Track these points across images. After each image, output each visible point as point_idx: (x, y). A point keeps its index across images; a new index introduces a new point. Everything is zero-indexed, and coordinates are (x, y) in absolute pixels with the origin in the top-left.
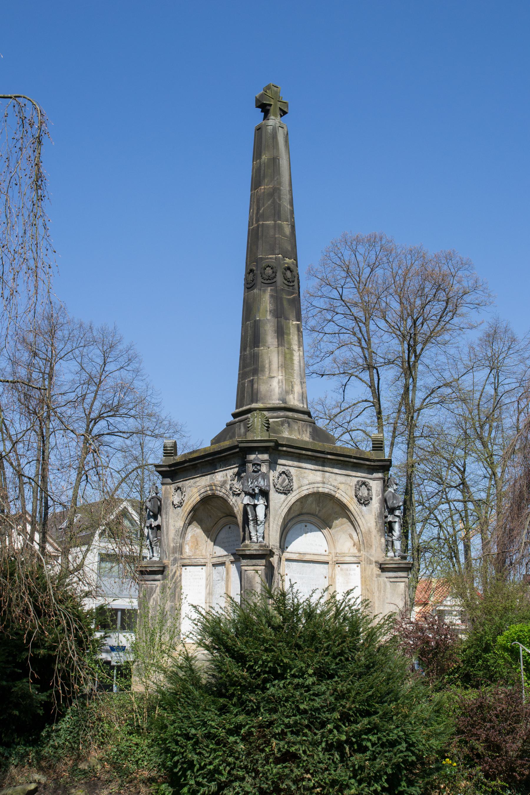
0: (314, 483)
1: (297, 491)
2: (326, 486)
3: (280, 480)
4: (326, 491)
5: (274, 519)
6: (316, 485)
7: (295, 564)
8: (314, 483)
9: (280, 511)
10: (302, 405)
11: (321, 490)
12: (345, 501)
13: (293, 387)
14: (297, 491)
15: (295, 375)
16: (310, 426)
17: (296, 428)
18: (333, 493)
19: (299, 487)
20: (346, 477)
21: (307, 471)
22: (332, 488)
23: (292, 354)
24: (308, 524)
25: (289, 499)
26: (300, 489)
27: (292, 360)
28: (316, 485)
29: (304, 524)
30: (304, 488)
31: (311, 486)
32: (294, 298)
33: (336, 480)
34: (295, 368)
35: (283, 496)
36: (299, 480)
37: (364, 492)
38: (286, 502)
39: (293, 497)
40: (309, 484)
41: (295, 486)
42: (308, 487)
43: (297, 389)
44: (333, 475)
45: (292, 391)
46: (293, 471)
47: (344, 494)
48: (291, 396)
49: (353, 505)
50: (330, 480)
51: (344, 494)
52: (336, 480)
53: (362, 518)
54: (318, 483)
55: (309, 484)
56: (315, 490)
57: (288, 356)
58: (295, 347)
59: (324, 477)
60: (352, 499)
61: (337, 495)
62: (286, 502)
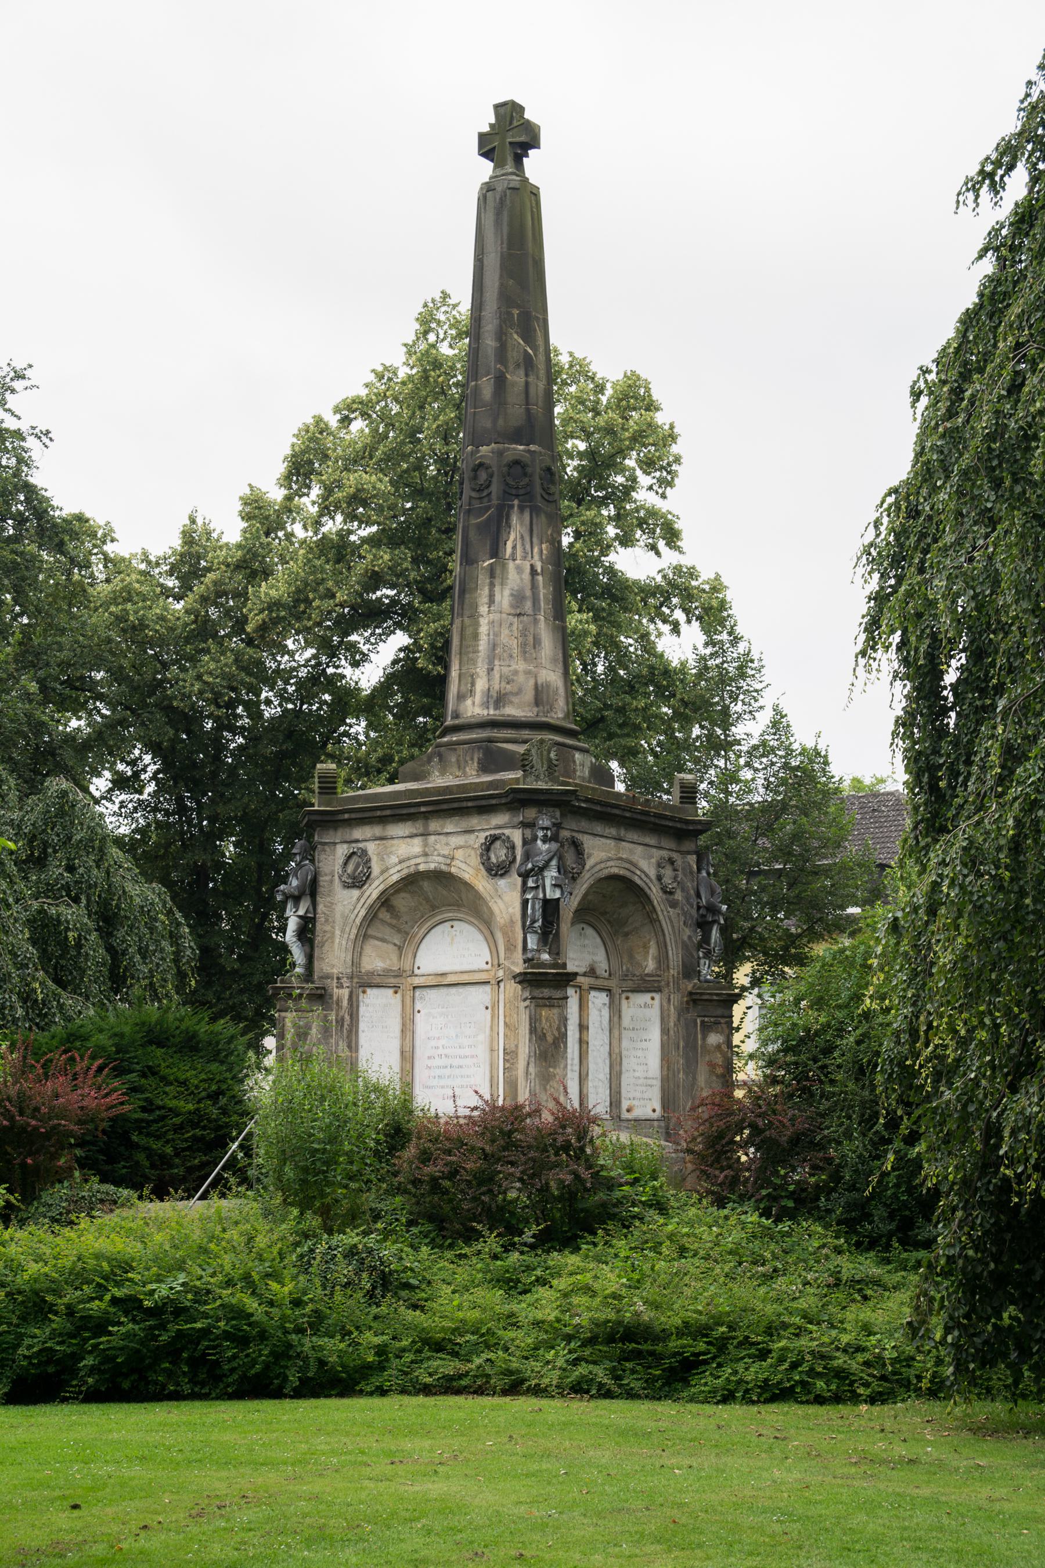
0: (409, 859)
1: (381, 879)
2: (430, 859)
3: (350, 868)
4: (432, 866)
5: (343, 931)
6: (413, 862)
7: (428, 990)
8: (409, 859)
9: (353, 916)
10: (485, 712)
11: (422, 868)
12: (466, 877)
13: (473, 684)
14: (381, 879)
15: (480, 660)
16: (479, 748)
17: (454, 759)
18: (444, 868)
19: (383, 872)
20: (467, 836)
21: (395, 842)
22: (441, 859)
23: (477, 625)
24: (455, 923)
25: (367, 893)
26: (386, 875)
27: (476, 636)
28: (413, 862)
29: (448, 924)
30: (392, 871)
31: (404, 865)
32: (489, 519)
33: (447, 844)
34: (481, 648)
35: (356, 893)
36: (382, 860)
37: (499, 854)
38: (362, 901)
39: (373, 891)
40: (400, 862)
41: (376, 869)
42: (398, 868)
43: (481, 685)
44: (442, 837)
45: (472, 692)
46: (371, 847)
47: (463, 866)
48: (469, 702)
49: (482, 883)
50: (438, 846)
51: (463, 866)
52: (447, 844)
53: (499, 901)
54: (416, 857)
55: (400, 862)
56: (412, 870)
57: (469, 631)
58: (483, 609)
59: (426, 845)
60: (478, 870)
61: (453, 870)
62: (362, 901)
